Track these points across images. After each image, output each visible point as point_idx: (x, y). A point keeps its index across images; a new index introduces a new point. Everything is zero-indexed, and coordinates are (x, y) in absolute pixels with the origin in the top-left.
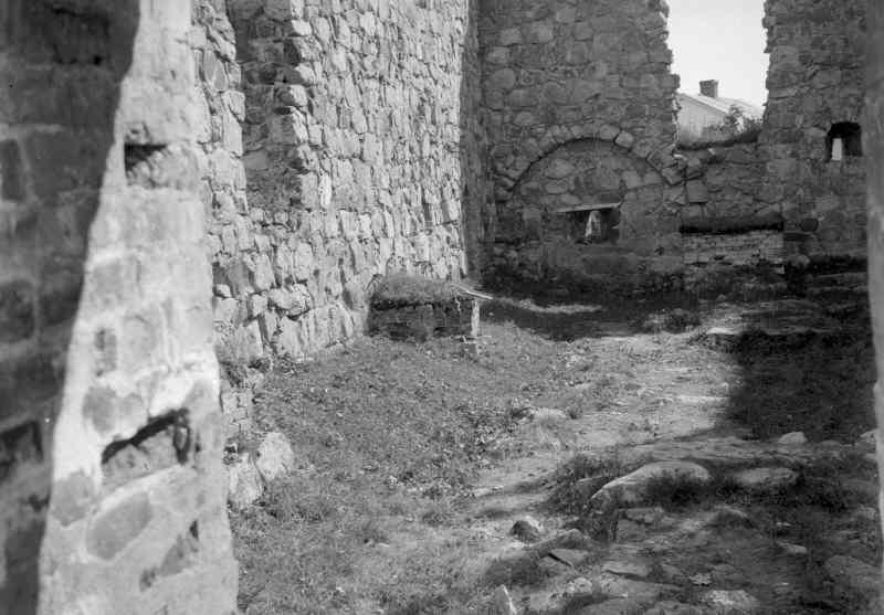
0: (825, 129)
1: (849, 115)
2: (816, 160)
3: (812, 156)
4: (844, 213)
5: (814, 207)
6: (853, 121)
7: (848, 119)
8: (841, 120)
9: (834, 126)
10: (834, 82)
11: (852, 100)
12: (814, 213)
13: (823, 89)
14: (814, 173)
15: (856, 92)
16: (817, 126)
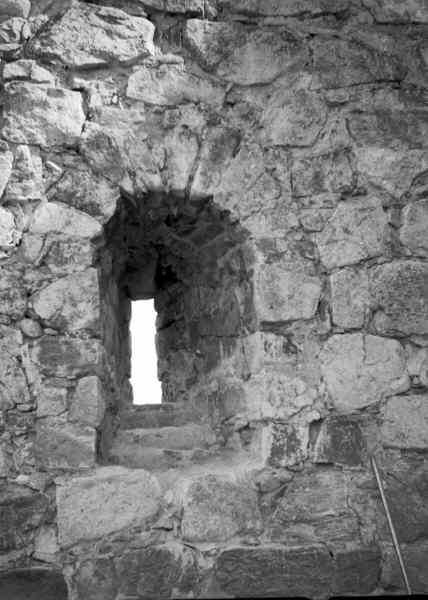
0: (93, 210)
1: (183, 162)
2: (60, 326)
3: (43, 307)
4: (174, 546)
5: (50, 520)
6: (197, 188)
7: (180, 184)
8: (156, 180)
9: (125, 199)
10: (122, 49)
11: (196, 120)
12: (46, 547)
13: (87, 70)
14: (47, 375)
15: (205, 91)
16: (68, 199)
